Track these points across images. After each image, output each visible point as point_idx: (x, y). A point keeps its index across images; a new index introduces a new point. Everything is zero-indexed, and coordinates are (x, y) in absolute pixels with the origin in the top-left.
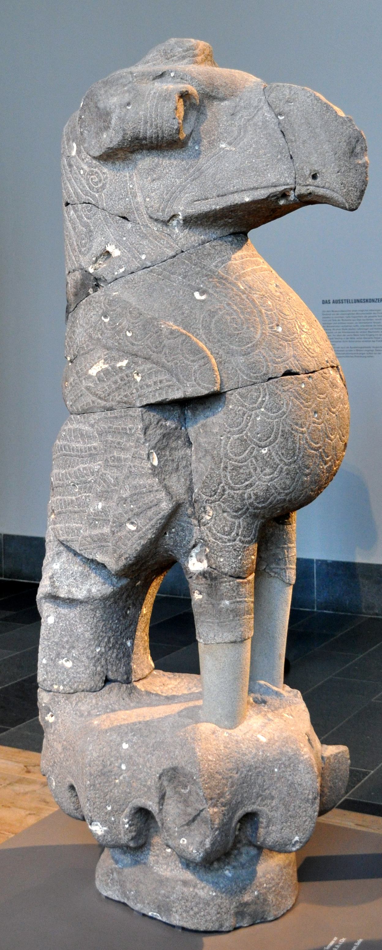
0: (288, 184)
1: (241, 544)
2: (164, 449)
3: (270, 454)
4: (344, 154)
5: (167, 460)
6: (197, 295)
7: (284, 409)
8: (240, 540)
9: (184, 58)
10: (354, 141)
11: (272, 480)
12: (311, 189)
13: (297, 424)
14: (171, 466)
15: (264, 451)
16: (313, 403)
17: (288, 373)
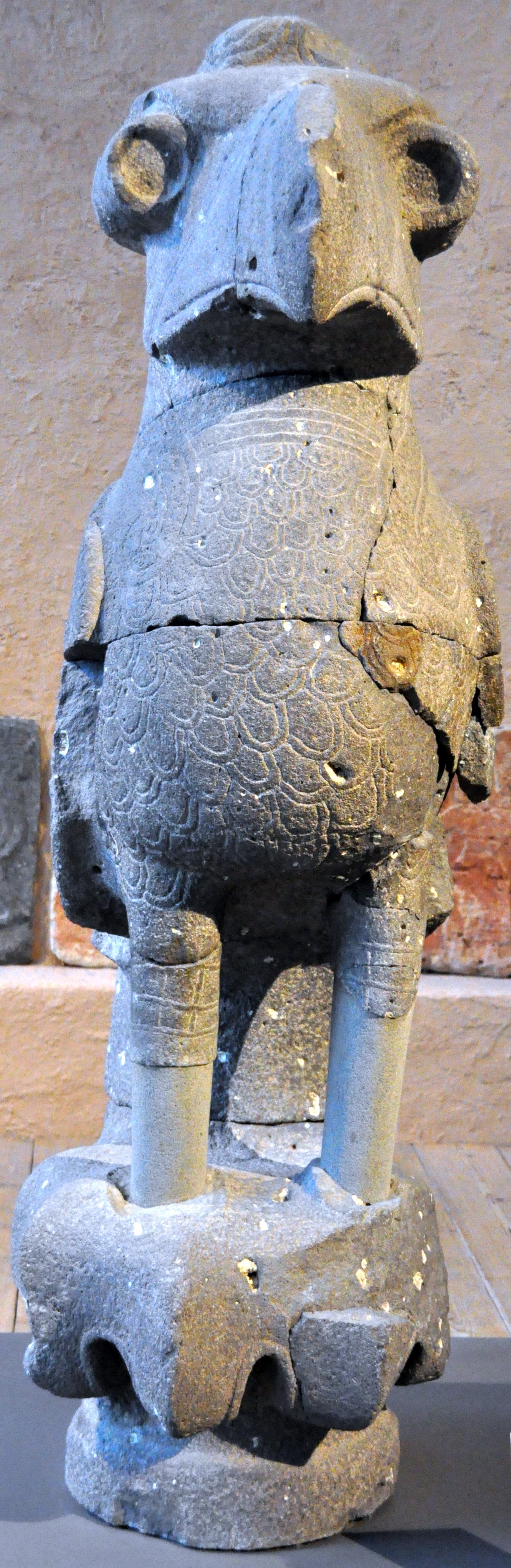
0: (228, 282)
1: (149, 905)
2: (83, 730)
3: (140, 756)
4: (284, 216)
5: (84, 749)
6: (149, 483)
7: (156, 681)
8: (147, 897)
9: (223, 58)
10: (299, 188)
11: (149, 800)
12: (250, 286)
13: (173, 711)
14: (86, 760)
15: (132, 750)
16: (210, 677)
17: (179, 621)
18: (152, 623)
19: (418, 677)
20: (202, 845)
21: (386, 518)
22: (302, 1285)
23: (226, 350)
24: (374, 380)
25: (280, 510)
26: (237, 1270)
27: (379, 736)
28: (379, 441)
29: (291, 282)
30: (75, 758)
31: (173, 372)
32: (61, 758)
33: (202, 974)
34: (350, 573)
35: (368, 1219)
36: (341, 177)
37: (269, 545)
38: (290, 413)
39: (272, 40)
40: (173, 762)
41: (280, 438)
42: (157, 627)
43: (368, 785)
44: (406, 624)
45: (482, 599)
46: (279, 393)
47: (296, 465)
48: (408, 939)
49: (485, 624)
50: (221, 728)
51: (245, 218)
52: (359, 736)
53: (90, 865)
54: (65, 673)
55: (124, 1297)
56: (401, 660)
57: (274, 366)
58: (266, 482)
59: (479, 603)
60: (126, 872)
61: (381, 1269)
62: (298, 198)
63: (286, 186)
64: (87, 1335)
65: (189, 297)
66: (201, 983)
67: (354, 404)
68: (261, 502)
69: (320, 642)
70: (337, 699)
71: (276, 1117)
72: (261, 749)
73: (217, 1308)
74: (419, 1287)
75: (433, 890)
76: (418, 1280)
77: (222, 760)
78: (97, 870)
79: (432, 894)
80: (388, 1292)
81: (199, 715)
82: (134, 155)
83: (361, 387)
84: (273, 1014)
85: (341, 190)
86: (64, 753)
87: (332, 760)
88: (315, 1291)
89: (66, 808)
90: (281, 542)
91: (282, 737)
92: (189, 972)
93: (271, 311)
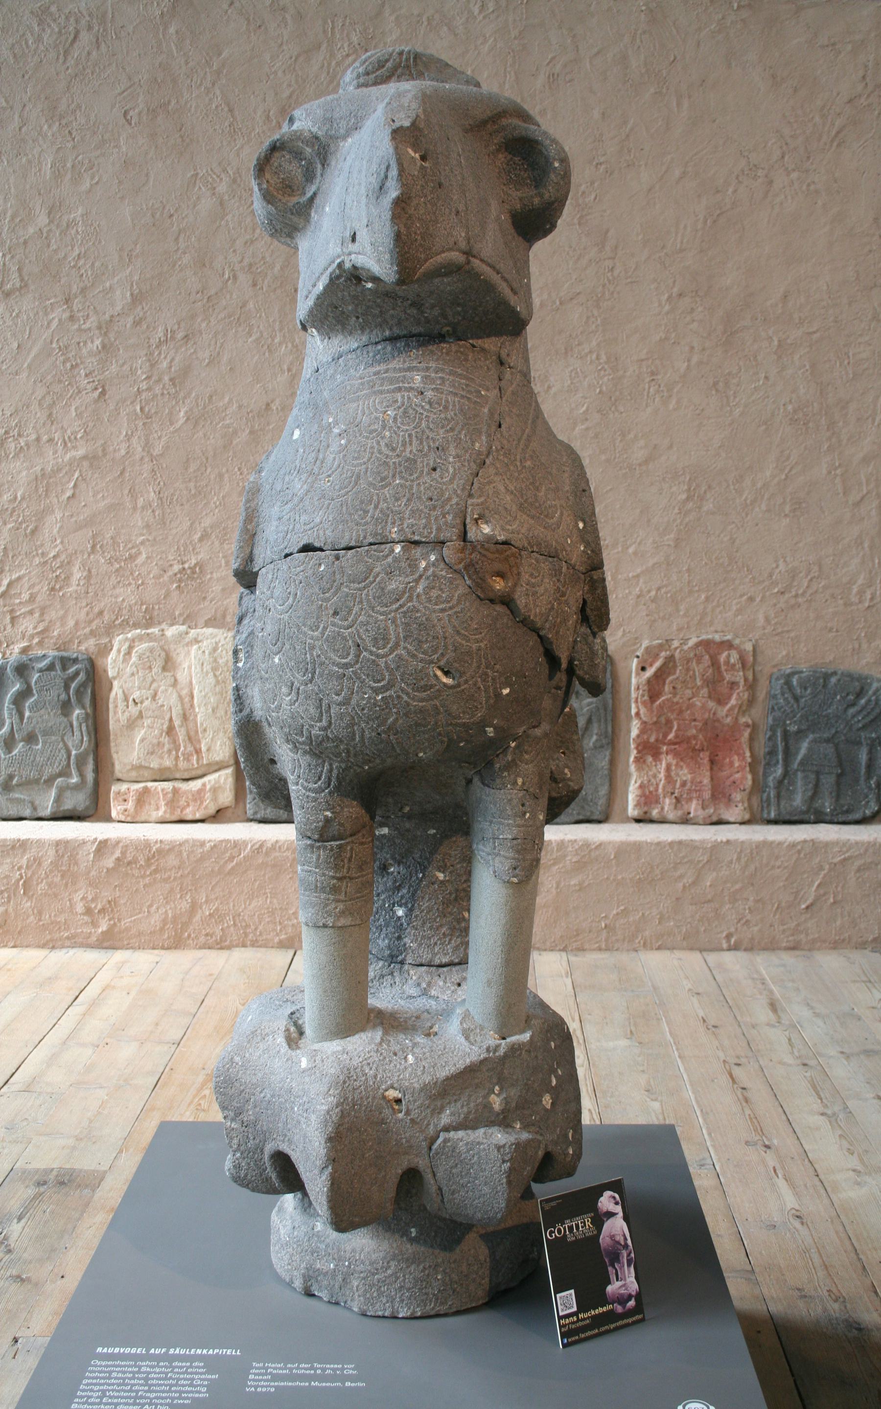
0: (339, 256)
8: (302, 786)
9: (350, 83)
10: (383, 167)
11: (292, 703)
17: (307, 548)
18: (287, 551)
19: (519, 589)
20: (338, 740)
21: (489, 454)
22: (442, 1110)
23: (354, 319)
24: (486, 340)
25: (393, 450)
26: (384, 1097)
27: (481, 641)
28: (487, 390)
29: (380, 248)
30: (249, 668)
31: (319, 343)
32: (238, 669)
33: (352, 849)
34: (455, 500)
35: (501, 1052)
36: (423, 158)
37: (383, 479)
38: (410, 369)
39: (389, 65)
40: (307, 669)
41: (399, 389)
42: (291, 554)
43: (475, 685)
44: (505, 543)
45: (584, 521)
46: (400, 352)
47: (411, 411)
48: (528, 815)
49: (587, 544)
50: (344, 638)
51: (349, 201)
52: (464, 642)
53: (266, 758)
54: (241, 598)
55: (293, 1119)
56: (501, 575)
57: (397, 331)
58: (384, 427)
59: (581, 525)
60: (290, 762)
61: (514, 1092)
62: (382, 175)
63: (374, 167)
64: (269, 1148)
65: (317, 275)
66: (351, 856)
67: (466, 360)
68: (378, 443)
69: (426, 561)
70: (443, 610)
71: (445, 960)
72: (378, 656)
73: (366, 1130)
74: (548, 1107)
75: (566, 771)
76: (547, 1100)
77: (346, 666)
78: (273, 762)
79: (566, 774)
80: (518, 1112)
81: (325, 628)
82: (276, 164)
83: (474, 346)
84: (441, 876)
85: (422, 168)
86: (240, 665)
87: (442, 663)
88: (452, 1114)
89: (241, 711)
90: (394, 476)
91: (397, 645)
92: (340, 847)
93: (375, 279)
